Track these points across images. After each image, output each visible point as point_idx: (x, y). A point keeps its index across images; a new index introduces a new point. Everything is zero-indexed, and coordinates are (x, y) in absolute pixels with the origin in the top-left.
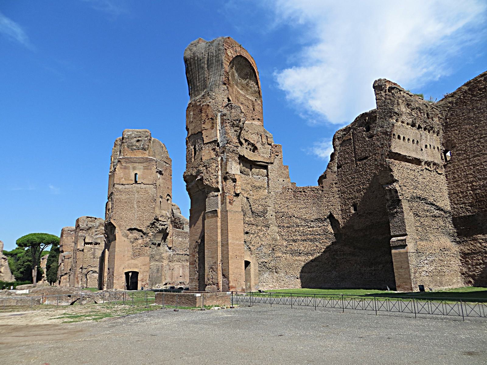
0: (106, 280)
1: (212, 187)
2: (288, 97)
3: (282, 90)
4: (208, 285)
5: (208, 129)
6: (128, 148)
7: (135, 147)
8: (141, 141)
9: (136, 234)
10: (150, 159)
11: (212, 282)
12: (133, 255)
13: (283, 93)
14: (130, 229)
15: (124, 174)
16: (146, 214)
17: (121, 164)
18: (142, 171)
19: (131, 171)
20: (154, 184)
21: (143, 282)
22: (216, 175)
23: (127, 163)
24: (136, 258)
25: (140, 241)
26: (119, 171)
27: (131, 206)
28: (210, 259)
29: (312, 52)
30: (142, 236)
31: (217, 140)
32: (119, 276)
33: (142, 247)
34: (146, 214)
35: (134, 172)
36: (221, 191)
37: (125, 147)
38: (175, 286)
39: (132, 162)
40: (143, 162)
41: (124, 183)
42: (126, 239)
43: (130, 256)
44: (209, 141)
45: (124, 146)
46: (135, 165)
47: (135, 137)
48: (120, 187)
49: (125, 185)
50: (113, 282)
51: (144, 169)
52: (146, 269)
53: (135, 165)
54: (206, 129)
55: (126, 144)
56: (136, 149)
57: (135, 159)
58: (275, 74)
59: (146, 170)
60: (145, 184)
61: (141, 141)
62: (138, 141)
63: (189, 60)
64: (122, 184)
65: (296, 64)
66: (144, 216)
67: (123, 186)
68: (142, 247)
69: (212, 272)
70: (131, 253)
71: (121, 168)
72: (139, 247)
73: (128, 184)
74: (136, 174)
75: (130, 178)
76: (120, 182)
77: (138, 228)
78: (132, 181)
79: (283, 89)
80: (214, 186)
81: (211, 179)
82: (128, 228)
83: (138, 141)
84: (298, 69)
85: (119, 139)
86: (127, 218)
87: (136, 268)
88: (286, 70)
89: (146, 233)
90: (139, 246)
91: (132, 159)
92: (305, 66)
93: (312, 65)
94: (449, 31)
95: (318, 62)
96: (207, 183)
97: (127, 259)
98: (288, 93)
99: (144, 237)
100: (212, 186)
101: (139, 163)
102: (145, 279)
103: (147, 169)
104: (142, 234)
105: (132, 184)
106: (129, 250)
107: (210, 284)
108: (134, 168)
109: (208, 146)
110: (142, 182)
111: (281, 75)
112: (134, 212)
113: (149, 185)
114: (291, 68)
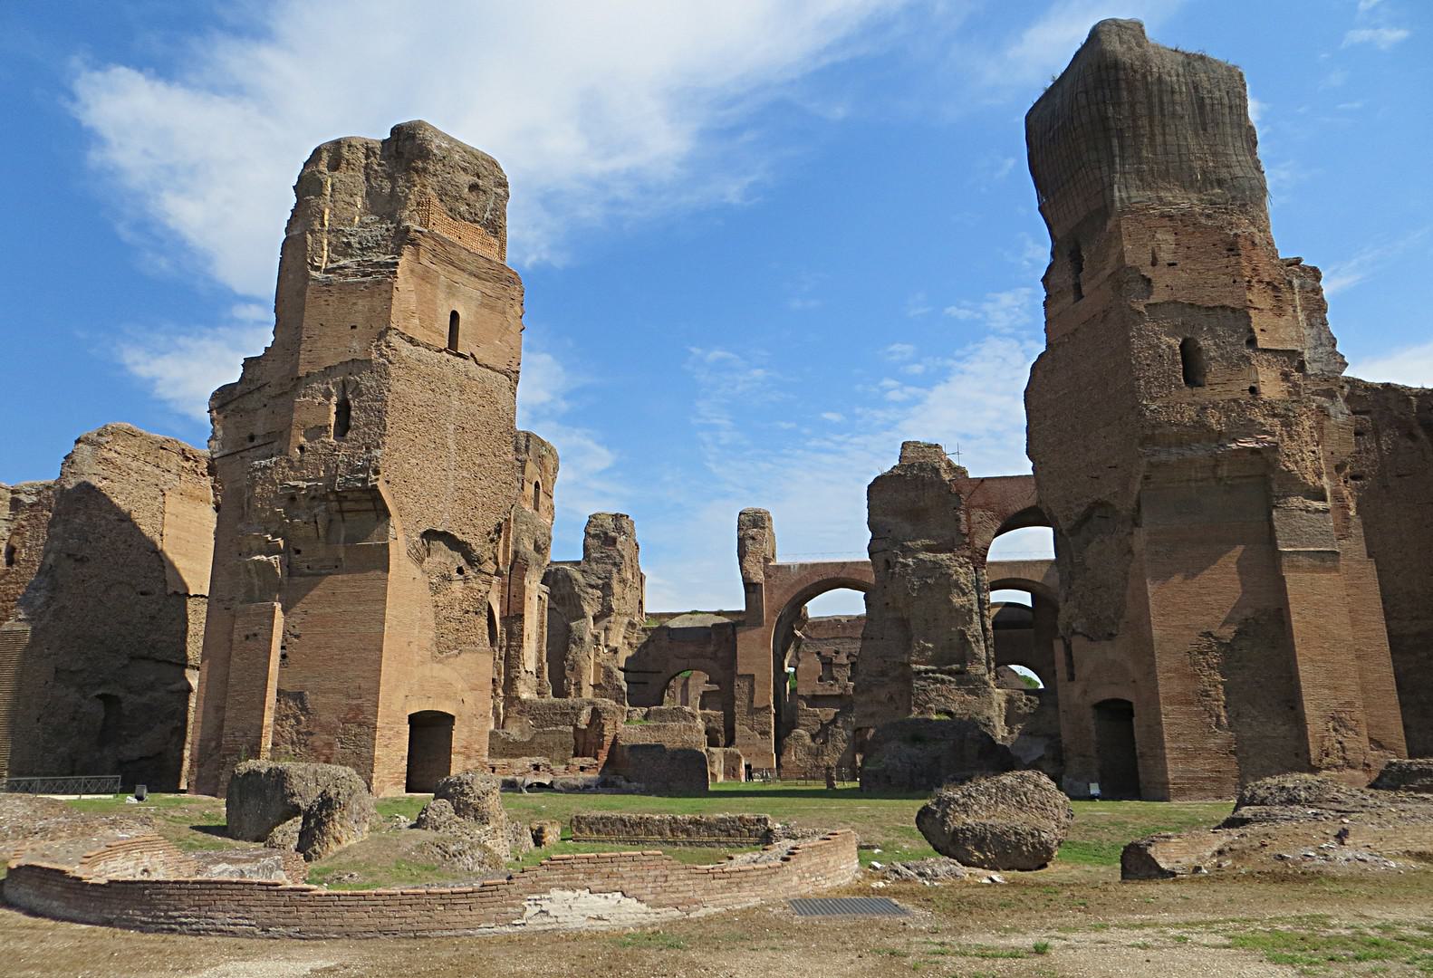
0: (270, 746)
1: (1305, 483)
2: (95, 157)
3: (77, 123)
4: (1327, 769)
5: (1262, 309)
6: (442, 200)
7: (463, 208)
8: (485, 192)
9: (444, 558)
10: (513, 276)
11: (1344, 758)
12: (437, 644)
13: (85, 137)
14: (430, 535)
15: (420, 302)
16: (485, 483)
17: (418, 255)
18: (473, 305)
19: (441, 296)
20: (513, 376)
21: (468, 757)
22: (1314, 452)
23: (434, 260)
24: (447, 657)
25: (457, 586)
26: (406, 281)
27: (437, 441)
28: (1327, 691)
29: (232, 57)
30: (460, 571)
31: (1303, 353)
32: (392, 729)
33: (467, 612)
34: (485, 483)
35: (451, 302)
36: (1329, 499)
37: (429, 190)
38: (517, 778)
39: (452, 263)
40: (484, 276)
41: (418, 337)
42: (417, 573)
43: (428, 645)
44: (1274, 348)
45: (424, 186)
46: (455, 278)
47: (464, 170)
48: (405, 349)
49: (419, 345)
50: (372, 758)
51: (482, 305)
52: (481, 704)
53: (461, 277)
54: (1258, 309)
55: (431, 180)
56: (467, 215)
57: (464, 254)
58: (75, 62)
59: (486, 311)
60: (480, 365)
61: (485, 192)
62: (474, 187)
63: (1125, 69)
64: (411, 341)
65: (163, 69)
66: (478, 490)
67: (412, 347)
68: (467, 612)
69: (1335, 730)
70: (432, 634)
71: (412, 271)
72: (457, 613)
73: (428, 347)
74: (454, 315)
75: (437, 326)
76: (406, 327)
77: (456, 534)
78: (443, 336)
79: (86, 123)
80: (1310, 479)
81: (1303, 460)
82: (424, 527)
83: (474, 187)
84: (160, 86)
85: (363, 145)
86: (422, 485)
87: (447, 697)
88: (122, 70)
89: (478, 560)
90: (457, 608)
91: (456, 251)
92: (186, 85)
93: (214, 89)
94: (596, 167)
95: (238, 91)
96: (1292, 467)
97: (418, 658)
98: (101, 142)
99: (470, 573)
100: (1304, 478)
101: (472, 274)
102: (477, 747)
103: (492, 308)
104: (462, 563)
105: (440, 351)
106: (425, 620)
107: (1336, 767)
108: (452, 290)
109: (1267, 360)
110: (472, 355)
111: (98, 76)
112: (445, 464)
113: (494, 374)
114: (140, 69)
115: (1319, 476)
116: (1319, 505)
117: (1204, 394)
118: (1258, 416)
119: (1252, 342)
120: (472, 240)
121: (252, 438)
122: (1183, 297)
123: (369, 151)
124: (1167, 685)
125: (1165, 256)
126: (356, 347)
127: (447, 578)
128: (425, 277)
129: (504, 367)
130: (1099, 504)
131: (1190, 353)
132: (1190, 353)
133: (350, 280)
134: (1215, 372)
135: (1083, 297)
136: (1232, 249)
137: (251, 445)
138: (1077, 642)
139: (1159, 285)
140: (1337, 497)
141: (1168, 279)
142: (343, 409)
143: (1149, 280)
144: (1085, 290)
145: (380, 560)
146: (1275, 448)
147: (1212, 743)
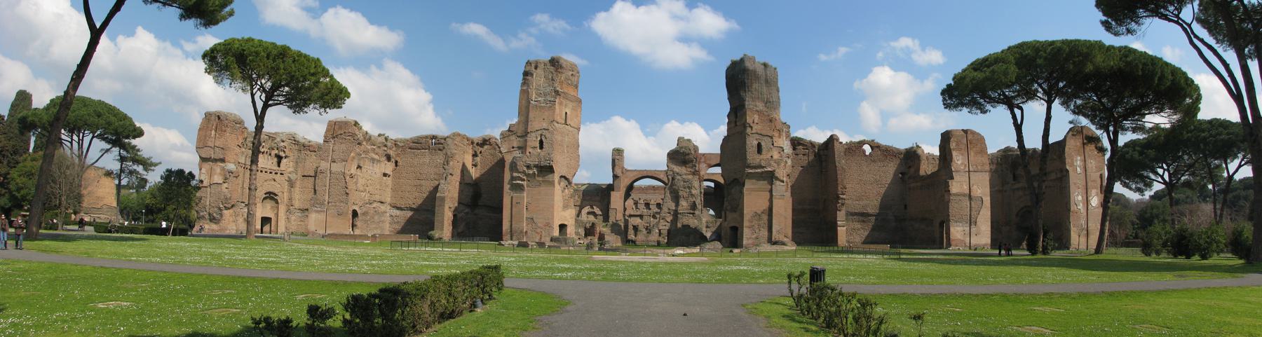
14: (561, 177)
53: (568, 102)
115: (783, 177)
116: (782, 184)
117: (762, 157)
118: (772, 163)
119: (773, 144)
120: (572, 92)
121: (513, 148)
122: (759, 132)
123: (545, 65)
124: (746, 223)
125: (756, 121)
126: (545, 125)
127: (565, 189)
128: (561, 104)
129: (576, 127)
130: (735, 179)
131: (759, 146)
132: (759, 146)
133: (542, 105)
134: (764, 152)
135: (736, 125)
136: (771, 121)
137: (512, 150)
138: (727, 212)
139: (754, 128)
140: (787, 182)
141: (756, 127)
142: (541, 142)
143: (751, 127)
144: (738, 124)
145: (552, 183)
146: (774, 171)
147: (753, 236)
